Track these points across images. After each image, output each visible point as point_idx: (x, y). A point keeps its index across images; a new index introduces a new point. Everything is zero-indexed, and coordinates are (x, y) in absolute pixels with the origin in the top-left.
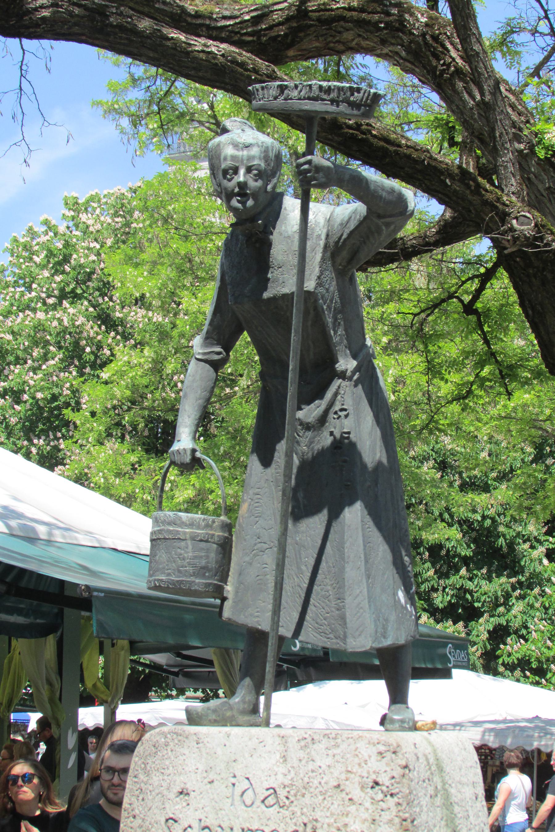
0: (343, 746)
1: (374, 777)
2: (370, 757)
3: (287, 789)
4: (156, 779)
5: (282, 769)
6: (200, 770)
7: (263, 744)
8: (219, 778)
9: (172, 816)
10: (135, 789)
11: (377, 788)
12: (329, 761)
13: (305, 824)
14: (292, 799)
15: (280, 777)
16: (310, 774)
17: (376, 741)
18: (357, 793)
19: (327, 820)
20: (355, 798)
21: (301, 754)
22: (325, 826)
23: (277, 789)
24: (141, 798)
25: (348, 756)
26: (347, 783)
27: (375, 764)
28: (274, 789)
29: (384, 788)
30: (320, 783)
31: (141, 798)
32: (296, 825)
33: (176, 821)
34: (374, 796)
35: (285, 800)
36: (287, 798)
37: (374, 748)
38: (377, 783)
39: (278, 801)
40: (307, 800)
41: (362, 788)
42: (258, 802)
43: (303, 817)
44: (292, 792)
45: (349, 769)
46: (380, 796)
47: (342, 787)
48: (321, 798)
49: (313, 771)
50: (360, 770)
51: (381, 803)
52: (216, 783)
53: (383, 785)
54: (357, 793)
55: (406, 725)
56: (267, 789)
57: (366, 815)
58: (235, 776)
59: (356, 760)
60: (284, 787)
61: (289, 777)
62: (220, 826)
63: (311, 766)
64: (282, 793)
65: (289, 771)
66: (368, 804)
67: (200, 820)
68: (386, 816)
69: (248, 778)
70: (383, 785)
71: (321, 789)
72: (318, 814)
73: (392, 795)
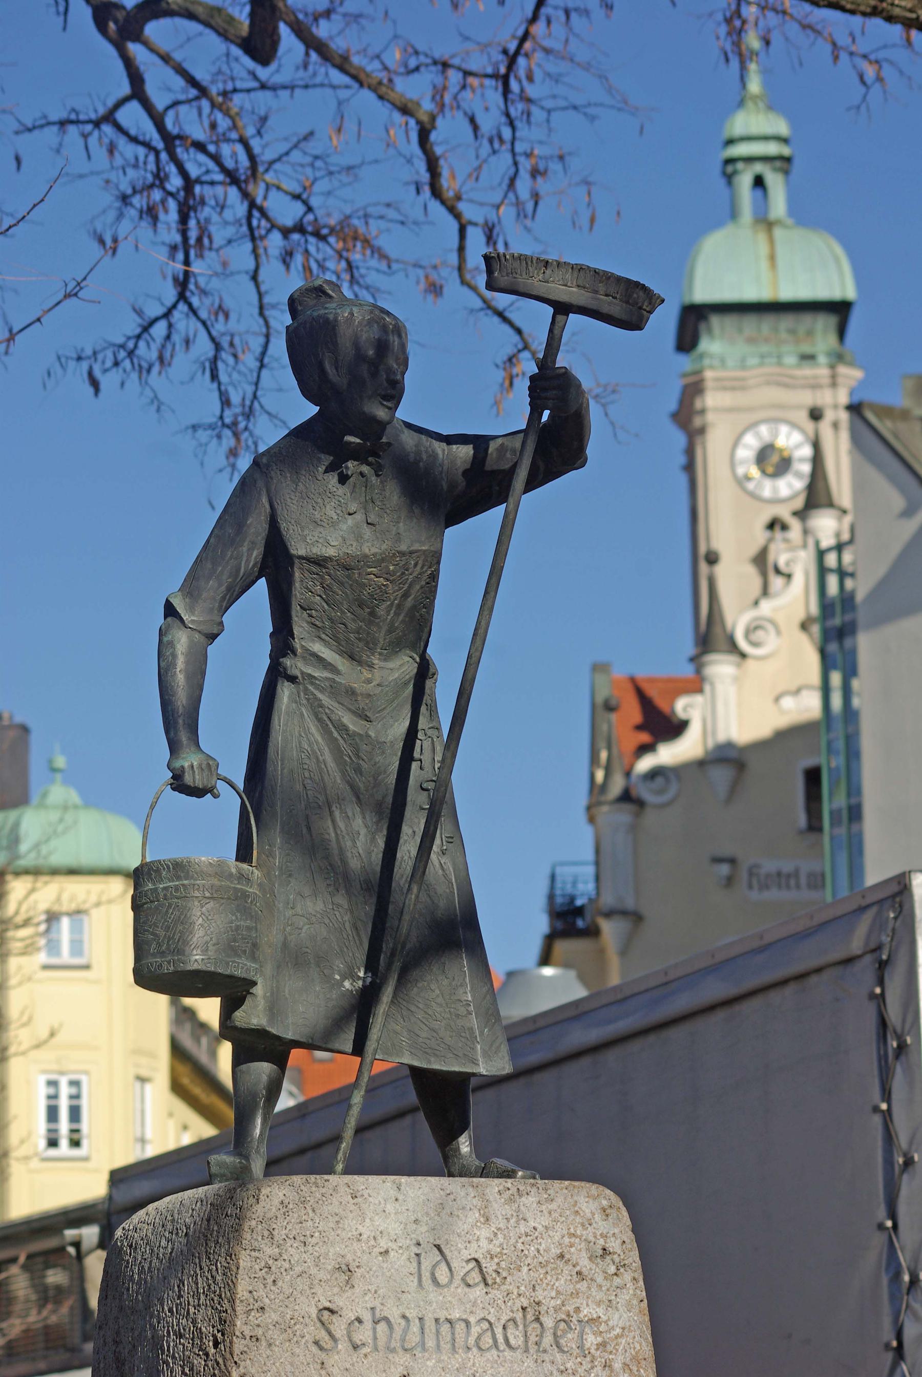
2: (593, 1214)
3: (496, 1260)
4: (293, 1252)
6: (364, 1237)
7: (452, 1197)
9: (328, 1305)
10: (257, 1267)
11: (608, 1258)
14: (504, 1274)
15: (484, 1243)
18: (585, 1263)
19: (553, 1303)
21: (508, 1210)
22: (551, 1311)
23: (483, 1261)
24: (270, 1281)
25: (568, 1212)
26: (573, 1250)
28: (476, 1260)
29: (617, 1260)
30: (538, 1251)
31: (270, 1281)
32: (512, 1311)
35: (494, 1275)
39: (484, 1280)
41: (590, 1258)
42: (457, 1281)
44: (503, 1264)
45: (572, 1230)
47: (567, 1256)
48: (542, 1271)
52: (392, 1254)
53: (615, 1253)
54: (585, 1263)
57: (599, 1296)
58: (419, 1244)
59: (578, 1219)
60: (492, 1258)
61: (497, 1242)
62: (404, 1317)
63: (522, 1228)
64: (489, 1267)
65: (495, 1234)
66: (600, 1279)
68: (625, 1296)
71: (541, 1259)
72: (540, 1295)
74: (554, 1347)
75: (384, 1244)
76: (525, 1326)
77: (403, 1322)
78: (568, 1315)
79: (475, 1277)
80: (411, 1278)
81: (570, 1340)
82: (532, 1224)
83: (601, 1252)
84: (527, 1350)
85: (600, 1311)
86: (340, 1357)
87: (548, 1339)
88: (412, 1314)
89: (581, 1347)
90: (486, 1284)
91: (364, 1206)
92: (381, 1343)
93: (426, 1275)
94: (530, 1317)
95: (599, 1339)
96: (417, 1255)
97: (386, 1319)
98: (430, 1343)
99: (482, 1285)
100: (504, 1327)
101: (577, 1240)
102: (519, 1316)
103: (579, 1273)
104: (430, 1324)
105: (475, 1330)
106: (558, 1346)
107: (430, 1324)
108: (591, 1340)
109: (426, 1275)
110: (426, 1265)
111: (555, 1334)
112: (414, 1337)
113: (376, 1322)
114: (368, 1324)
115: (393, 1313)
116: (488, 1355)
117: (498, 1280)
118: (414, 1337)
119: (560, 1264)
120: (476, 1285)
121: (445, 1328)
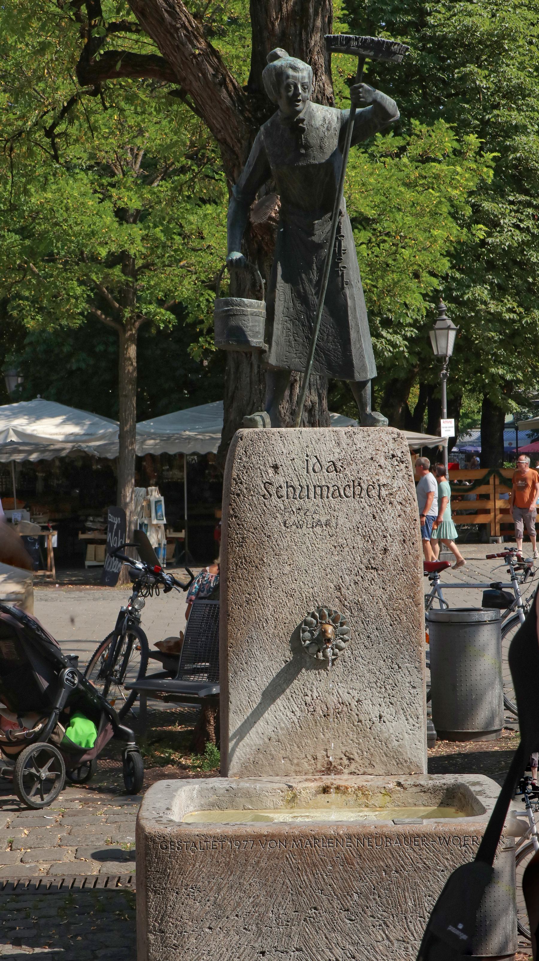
15: (336, 455)
20: (382, 465)
27: (391, 445)
38: (393, 456)
40: (354, 466)
41: (386, 459)
42: (325, 471)
46: (396, 463)
54: (382, 461)
57: (389, 474)
58: (307, 456)
64: (339, 464)
68: (400, 474)
73: (402, 462)
85: (389, 481)
87: (364, 493)
88: (304, 484)
89: (379, 496)
92: (291, 495)
93: (311, 469)
94: (356, 484)
97: (291, 486)
98: (312, 495)
100: (345, 489)
102: (352, 484)
103: (380, 466)
104: (312, 488)
106: (368, 495)
107: (312, 488)
108: (384, 492)
109: (311, 469)
114: (285, 489)
119: (371, 461)
121: (318, 490)
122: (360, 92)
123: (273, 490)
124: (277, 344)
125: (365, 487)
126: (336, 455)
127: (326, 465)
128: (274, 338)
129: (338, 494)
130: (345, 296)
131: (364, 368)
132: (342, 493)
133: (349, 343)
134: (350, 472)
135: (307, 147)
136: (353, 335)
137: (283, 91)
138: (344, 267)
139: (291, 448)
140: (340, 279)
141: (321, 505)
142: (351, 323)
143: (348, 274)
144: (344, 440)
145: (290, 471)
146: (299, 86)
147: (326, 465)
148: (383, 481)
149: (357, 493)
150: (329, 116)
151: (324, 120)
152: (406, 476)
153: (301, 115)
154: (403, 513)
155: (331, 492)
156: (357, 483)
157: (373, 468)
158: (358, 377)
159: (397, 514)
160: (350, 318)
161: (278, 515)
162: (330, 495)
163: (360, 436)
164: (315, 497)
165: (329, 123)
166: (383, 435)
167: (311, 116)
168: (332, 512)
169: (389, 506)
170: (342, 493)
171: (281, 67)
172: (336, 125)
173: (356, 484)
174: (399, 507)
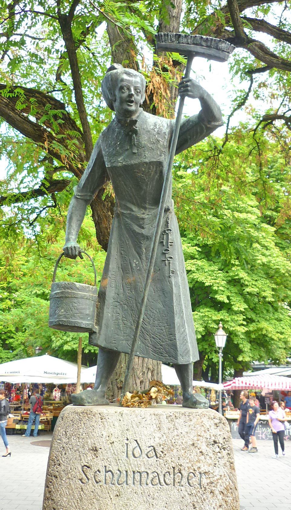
0: (194, 420)
1: (213, 438)
3: (162, 447)
5: (158, 435)
6: (104, 436)
7: (144, 420)
8: (117, 440)
9: (86, 464)
11: (216, 445)
12: (186, 429)
13: (174, 468)
14: (165, 453)
15: (157, 439)
16: (176, 437)
17: (213, 417)
20: (204, 451)
22: (186, 468)
23: (156, 447)
24: (63, 453)
26: (199, 442)
27: (214, 431)
29: (220, 445)
31: (63, 453)
33: (88, 467)
34: (214, 450)
35: (161, 453)
36: (162, 452)
37: (212, 421)
38: (215, 442)
42: (144, 455)
43: (172, 463)
45: (199, 434)
46: (218, 450)
47: (195, 445)
48: (183, 451)
49: (178, 436)
50: (205, 434)
51: (218, 454)
52: (115, 443)
53: (219, 443)
54: (204, 448)
55: (206, 405)
56: (149, 447)
57: (210, 462)
58: (127, 439)
62: (119, 470)
63: (175, 433)
64: (159, 449)
65: (163, 436)
66: (211, 455)
67: (105, 467)
68: (222, 462)
69: (136, 441)
70: (219, 443)
71: (183, 446)
72: (181, 462)
73: (224, 449)
74: (187, 484)
75: (113, 439)
76: (174, 475)
77: (118, 472)
78: (195, 470)
79: (152, 454)
80: (123, 454)
81: (194, 481)
82: (180, 431)
83: (213, 443)
84: (174, 485)
85: (210, 469)
86: (90, 485)
87: (185, 480)
88: (123, 469)
89: (200, 484)
90: (157, 457)
91: (105, 423)
92: (109, 481)
93: (130, 453)
94: (176, 471)
95: (209, 481)
96: (127, 444)
97: (110, 471)
98: (130, 481)
99: (155, 457)
101: (201, 438)
102: (172, 470)
105: (151, 476)
108: (205, 481)
109: (130, 453)
110: (130, 448)
111: (188, 478)
112: (123, 479)
113: (106, 472)
115: (114, 469)
116: (155, 487)
117: (162, 455)
118: (123, 479)
119: (192, 447)
120: (153, 457)
121: (137, 476)
122: (187, 86)
123: (90, 474)
124: (107, 327)
125: (185, 474)
126: (157, 439)
127: (146, 450)
128: (104, 322)
129: (158, 480)
130: (171, 283)
131: (187, 352)
132: (162, 481)
133: (174, 327)
134: (171, 459)
135: (139, 146)
136: (177, 320)
137: (117, 92)
138: (171, 258)
139: (112, 430)
140: (167, 268)
141: (139, 491)
142: (176, 309)
143: (173, 264)
144: (166, 424)
145: (109, 455)
146: (132, 89)
147: (146, 450)
148: (204, 469)
149: (177, 481)
150: (160, 122)
151: (155, 125)
152: (228, 464)
153: (134, 118)
154: (224, 503)
155: (150, 478)
156: (177, 470)
157: (194, 454)
158: (181, 361)
159: (218, 504)
160: (175, 304)
161: (95, 500)
162: (149, 482)
163: (181, 421)
164: (134, 483)
165: (159, 128)
166: (205, 420)
167: (145, 122)
168: (151, 500)
169: (210, 496)
170: (162, 481)
171: (117, 73)
172: (166, 130)
173: (176, 471)
174: (220, 497)
